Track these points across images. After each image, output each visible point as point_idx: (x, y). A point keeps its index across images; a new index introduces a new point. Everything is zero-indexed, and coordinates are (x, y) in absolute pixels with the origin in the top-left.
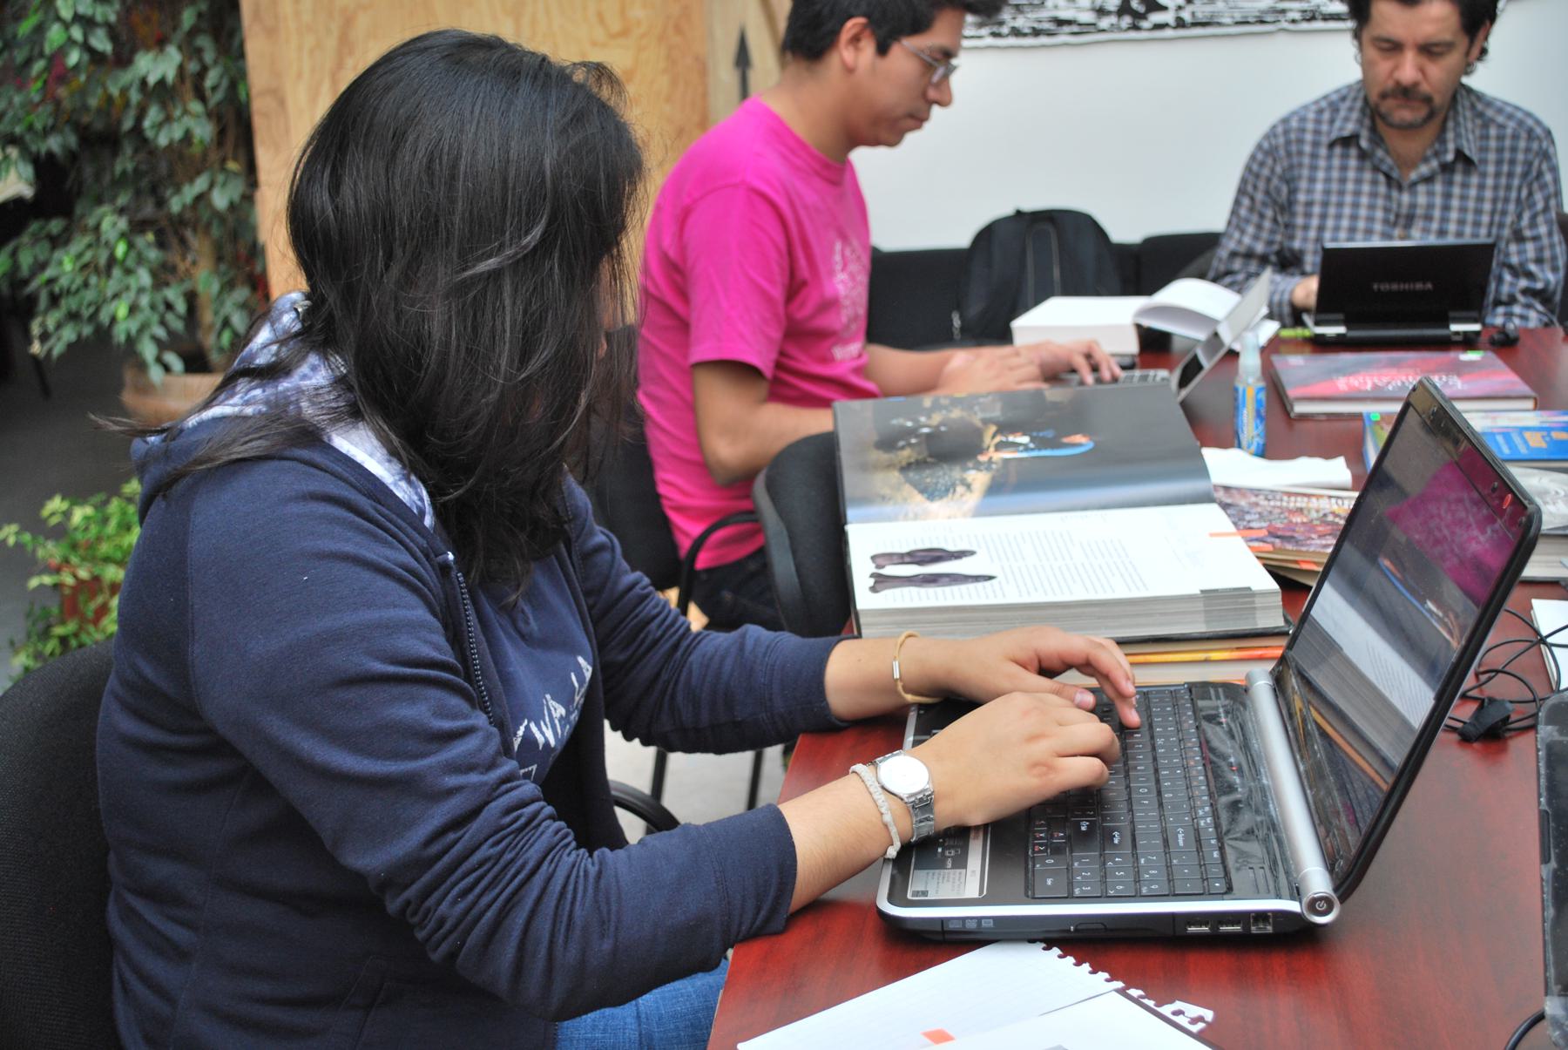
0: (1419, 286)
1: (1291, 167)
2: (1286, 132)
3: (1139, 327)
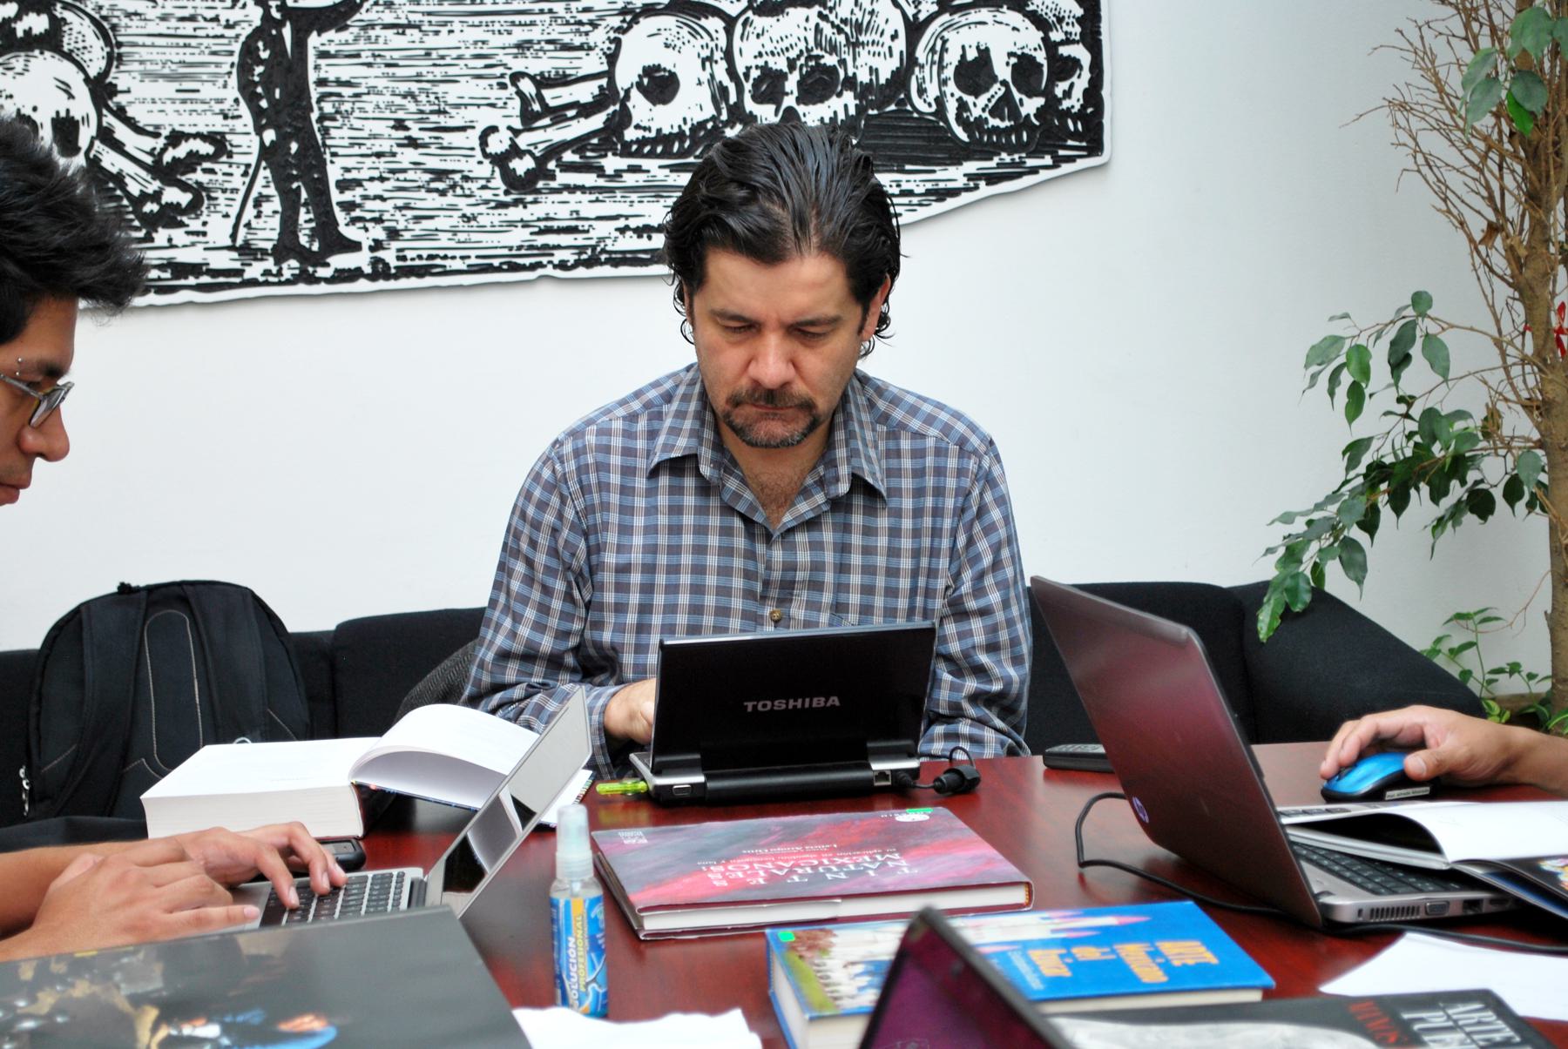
0: (819, 702)
1: (589, 510)
2: (578, 453)
3: (360, 788)
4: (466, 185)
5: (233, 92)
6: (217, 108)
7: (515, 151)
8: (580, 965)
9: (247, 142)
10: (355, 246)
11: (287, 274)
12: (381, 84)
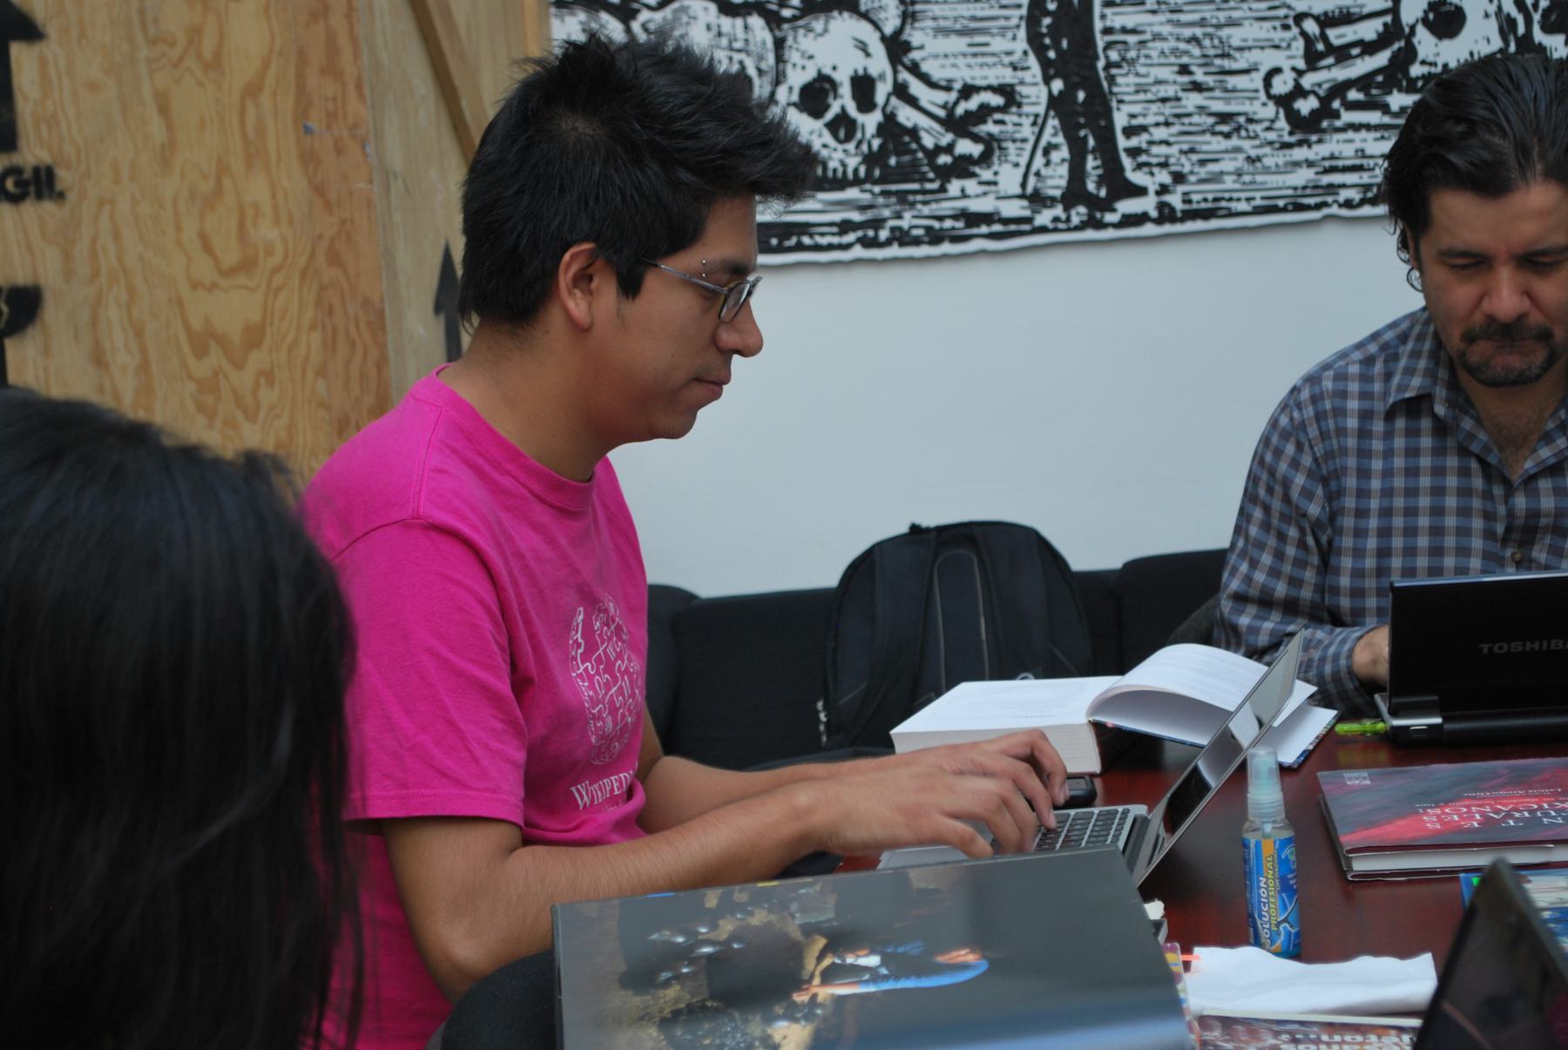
1: (1330, 455)
2: (1315, 399)
3: (1098, 727)
4: (1251, 127)
5: (1021, 44)
6: (1007, 60)
7: (1299, 92)
8: (1270, 904)
9: (1036, 92)
10: (1141, 191)
11: (1075, 220)
12: (1166, 30)
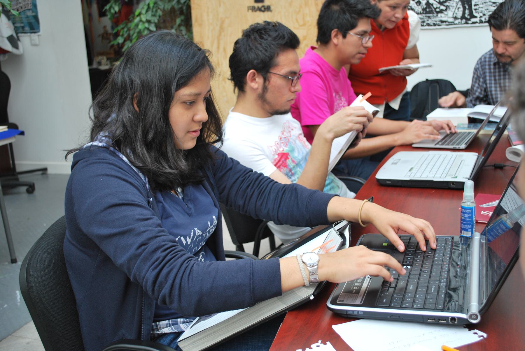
10: (476, 17)
